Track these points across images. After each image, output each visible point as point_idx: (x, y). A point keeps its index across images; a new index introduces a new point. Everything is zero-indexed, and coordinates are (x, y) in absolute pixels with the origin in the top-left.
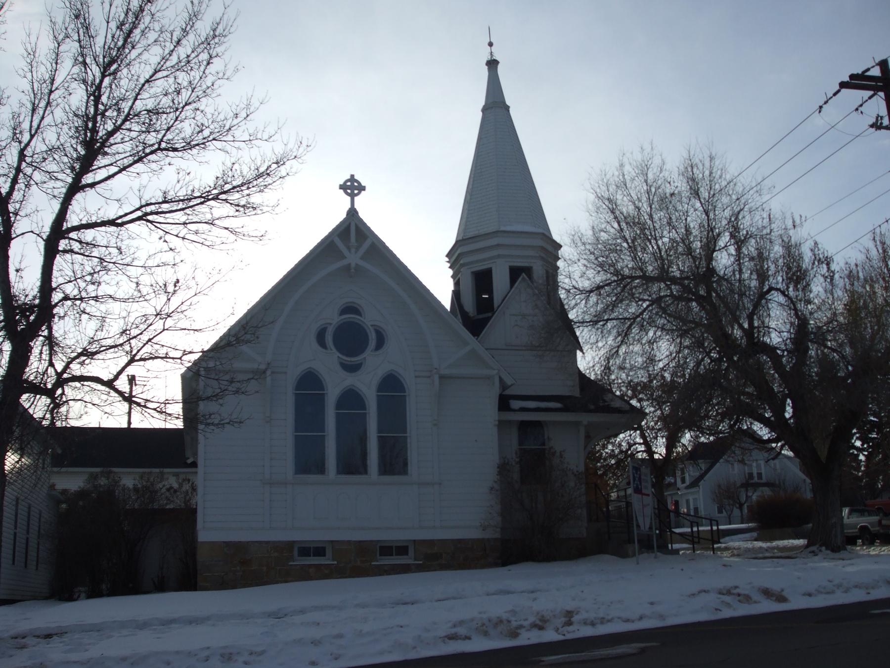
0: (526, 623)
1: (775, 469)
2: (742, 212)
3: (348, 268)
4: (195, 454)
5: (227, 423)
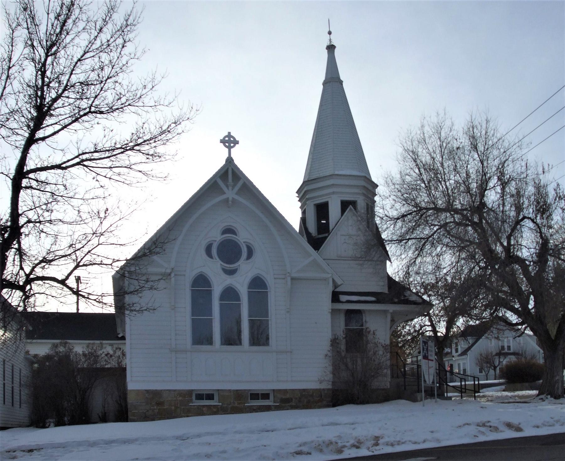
0: (348, 444)
1: (519, 344)
2: (507, 161)
3: (227, 200)
4: (124, 331)
5: (145, 310)
